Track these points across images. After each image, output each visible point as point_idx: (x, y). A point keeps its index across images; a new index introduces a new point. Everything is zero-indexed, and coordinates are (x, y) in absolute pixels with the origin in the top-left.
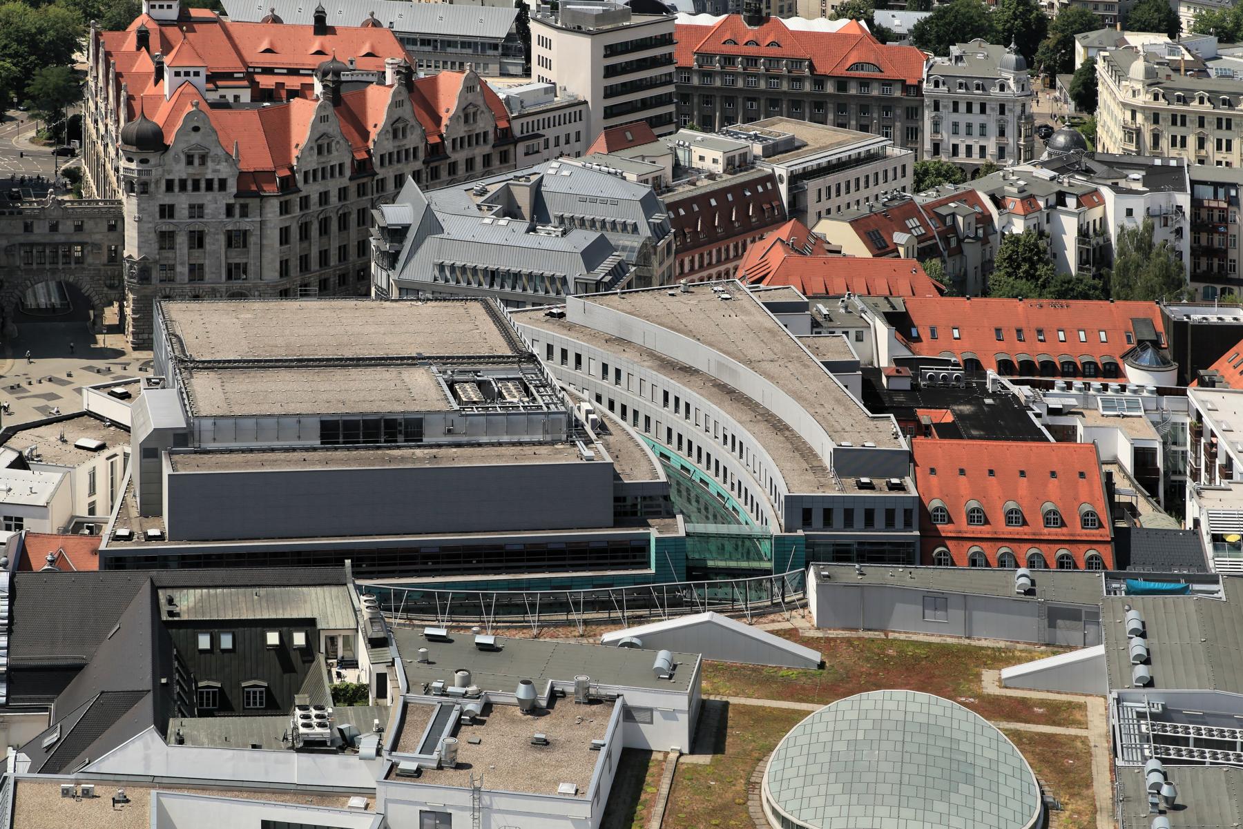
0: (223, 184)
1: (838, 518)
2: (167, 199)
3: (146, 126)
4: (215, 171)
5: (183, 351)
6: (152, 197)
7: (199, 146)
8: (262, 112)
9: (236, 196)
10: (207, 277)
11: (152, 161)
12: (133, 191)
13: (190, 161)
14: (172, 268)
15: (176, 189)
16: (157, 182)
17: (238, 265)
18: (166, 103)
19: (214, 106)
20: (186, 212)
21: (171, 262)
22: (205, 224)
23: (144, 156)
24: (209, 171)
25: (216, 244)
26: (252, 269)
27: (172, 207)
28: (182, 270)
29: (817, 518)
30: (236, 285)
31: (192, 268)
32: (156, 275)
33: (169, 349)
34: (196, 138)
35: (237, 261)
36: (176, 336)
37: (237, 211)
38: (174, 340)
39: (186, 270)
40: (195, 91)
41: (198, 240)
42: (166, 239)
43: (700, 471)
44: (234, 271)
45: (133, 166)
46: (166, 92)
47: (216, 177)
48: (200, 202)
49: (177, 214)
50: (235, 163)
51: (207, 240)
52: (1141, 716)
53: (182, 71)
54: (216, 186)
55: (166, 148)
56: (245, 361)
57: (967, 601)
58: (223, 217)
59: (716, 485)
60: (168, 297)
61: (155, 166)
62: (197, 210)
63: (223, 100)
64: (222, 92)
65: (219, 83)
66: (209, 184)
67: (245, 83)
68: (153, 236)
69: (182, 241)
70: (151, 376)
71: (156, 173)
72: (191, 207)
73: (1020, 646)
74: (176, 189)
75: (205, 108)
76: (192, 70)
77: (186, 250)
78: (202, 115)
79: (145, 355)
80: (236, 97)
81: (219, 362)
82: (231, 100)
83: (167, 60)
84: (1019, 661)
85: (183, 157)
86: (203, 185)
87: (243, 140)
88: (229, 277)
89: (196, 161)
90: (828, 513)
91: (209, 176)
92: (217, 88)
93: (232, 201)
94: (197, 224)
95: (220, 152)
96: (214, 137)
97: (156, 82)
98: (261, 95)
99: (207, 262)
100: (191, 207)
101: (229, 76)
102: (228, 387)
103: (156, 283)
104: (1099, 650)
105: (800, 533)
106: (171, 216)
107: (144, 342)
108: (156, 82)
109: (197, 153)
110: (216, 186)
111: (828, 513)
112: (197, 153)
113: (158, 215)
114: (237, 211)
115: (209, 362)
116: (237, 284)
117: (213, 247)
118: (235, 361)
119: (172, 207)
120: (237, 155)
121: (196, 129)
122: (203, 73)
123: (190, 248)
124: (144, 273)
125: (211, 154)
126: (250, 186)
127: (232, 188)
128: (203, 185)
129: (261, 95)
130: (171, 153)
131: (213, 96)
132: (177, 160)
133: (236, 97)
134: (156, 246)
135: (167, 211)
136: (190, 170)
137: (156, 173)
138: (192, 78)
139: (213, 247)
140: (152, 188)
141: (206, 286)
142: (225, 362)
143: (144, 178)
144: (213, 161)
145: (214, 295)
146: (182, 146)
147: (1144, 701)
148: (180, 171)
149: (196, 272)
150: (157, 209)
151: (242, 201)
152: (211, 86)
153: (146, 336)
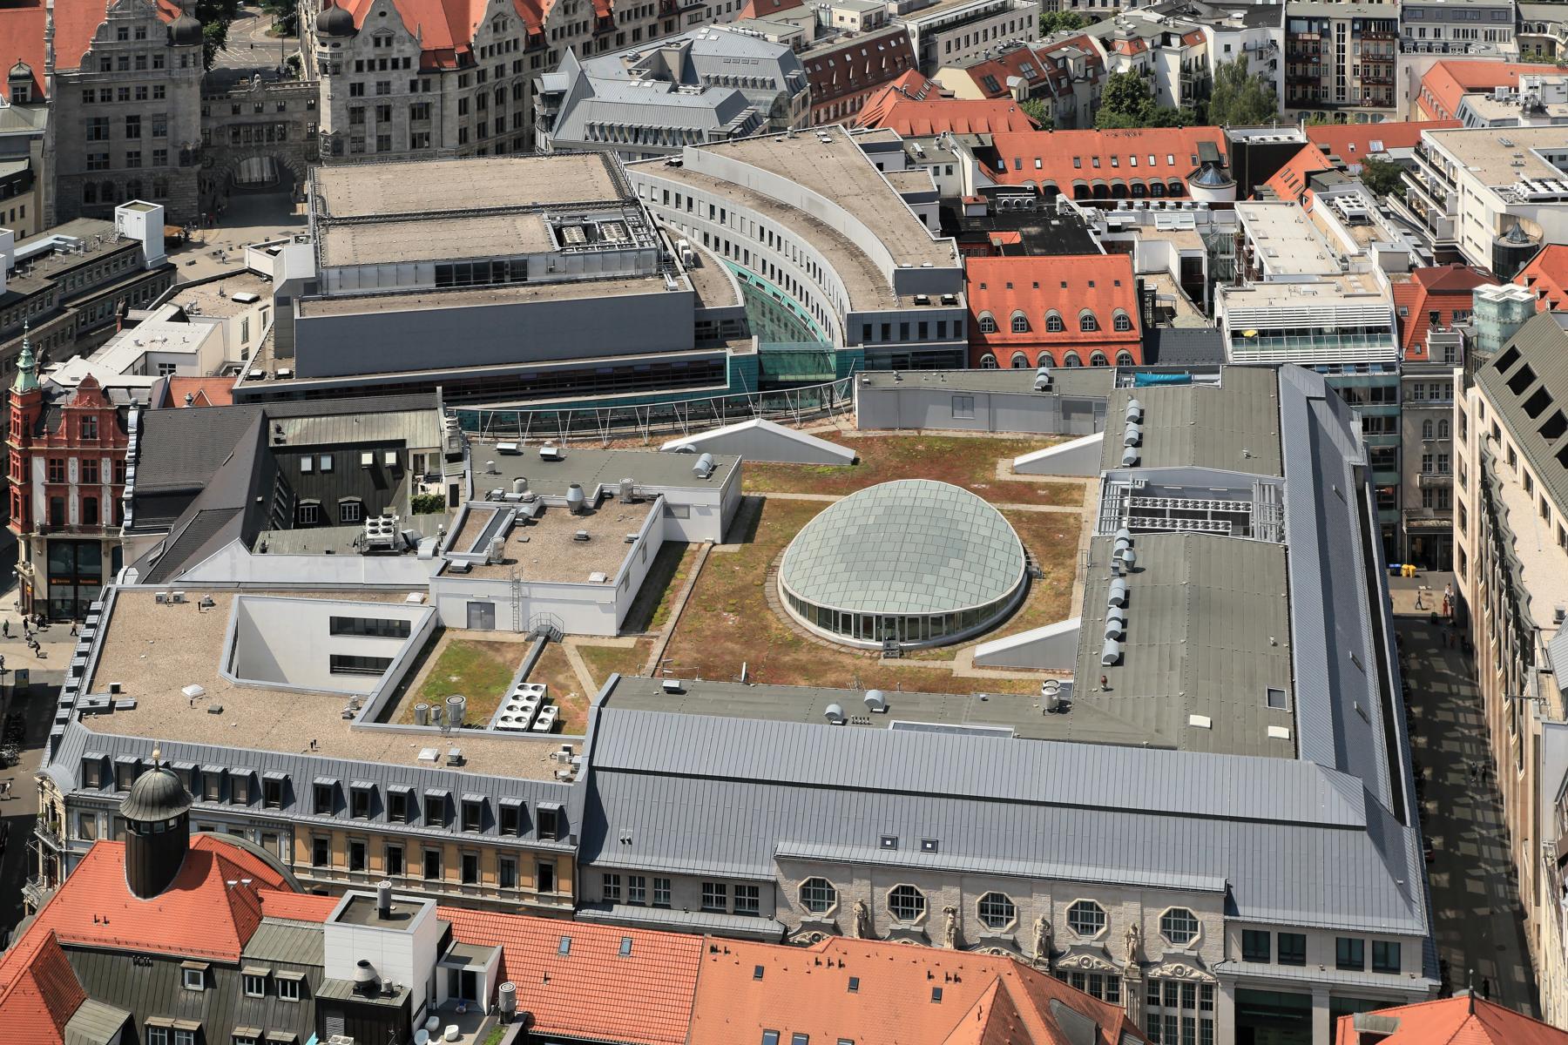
1: (895, 332)
26: (433, 138)
29: (877, 332)
43: (789, 297)
51: (394, 114)
52: (1125, 492)
57: (991, 400)
59: (801, 308)
69: (371, 116)
73: (1037, 437)
84: (1034, 449)
90: (886, 329)
104: (1099, 437)
105: (861, 346)
111: (886, 329)
147: (1130, 479)
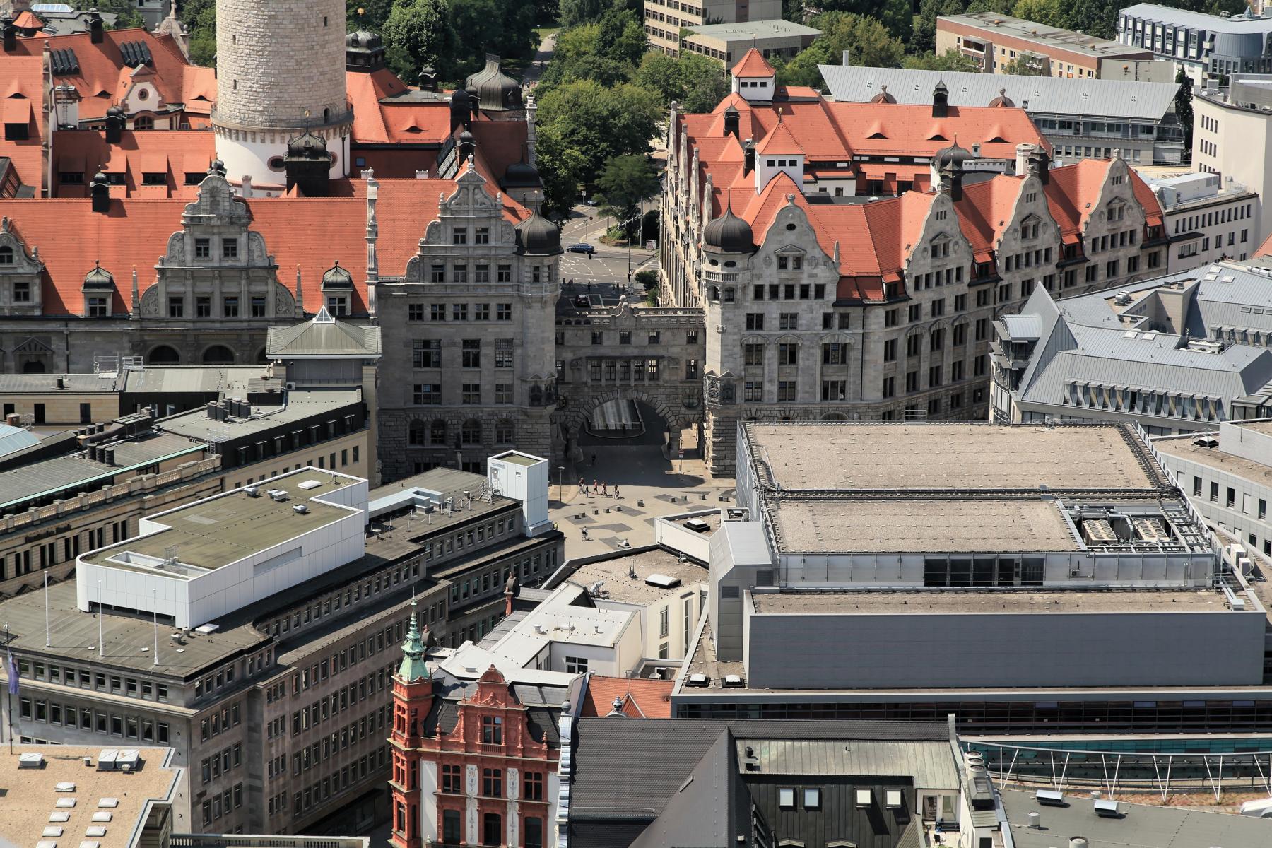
0: (820, 291)
2: (755, 308)
3: (734, 225)
4: (811, 276)
5: (770, 479)
6: (738, 306)
7: (793, 247)
8: (868, 207)
9: (834, 305)
10: (799, 396)
11: (740, 264)
12: (716, 298)
13: (783, 265)
14: (760, 386)
15: (767, 296)
16: (745, 288)
17: (834, 384)
18: (758, 197)
19: (812, 200)
20: (777, 323)
21: (759, 379)
22: (799, 336)
23: (730, 258)
24: (805, 276)
25: (810, 359)
27: (760, 317)
28: (771, 389)
30: (832, 406)
31: (782, 385)
32: (740, 393)
33: (754, 477)
34: (790, 237)
35: (834, 379)
36: (762, 463)
37: (836, 322)
38: (760, 467)
39: (775, 388)
40: (791, 183)
41: (789, 354)
42: (753, 353)
44: (830, 390)
45: (717, 269)
46: (758, 184)
47: (813, 283)
48: (793, 311)
49: (766, 325)
50: (835, 267)
53: (777, 159)
54: (812, 292)
55: (756, 249)
56: (840, 492)
58: (819, 328)
60: (754, 419)
61: (743, 269)
62: (789, 321)
63: (823, 194)
64: (821, 184)
65: (819, 174)
66: (805, 292)
67: (850, 174)
68: (738, 350)
70: (733, 507)
71: (743, 278)
72: (783, 316)
74: (767, 296)
75: (801, 201)
76: (788, 159)
77: (775, 366)
78: (798, 211)
79: (727, 483)
80: (839, 191)
81: (811, 492)
82: (832, 194)
83: (759, 147)
85: (775, 260)
86: (797, 292)
87: (845, 239)
88: (825, 396)
89: (790, 264)
91: (805, 282)
92: (817, 179)
93: (830, 310)
94: (789, 337)
95: (817, 253)
96: (812, 237)
97: (746, 173)
98: (869, 188)
99: (799, 379)
100: (783, 316)
101: (831, 165)
102: (821, 520)
103: (741, 402)
106: (760, 327)
107: (725, 469)
108: (746, 173)
109: (791, 255)
110: (812, 292)
112: (791, 255)
113: (744, 326)
114: (836, 322)
115: (799, 492)
116: (834, 404)
117: (807, 363)
118: (829, 492)
119: (760, 317)
120: (838, 258)
121: (791, 227)
122: (801, 162)
123: (781, 363)
124: (727, 392)
125: (808, 256)
126: (852, 293)
127: (831, 295)
128: (797, 292)
129: (869, 188)
130: (761, 255)
131: (812, 190)
132: (768, 263)
133: (839, 191)
134: (741, 361)
135: (755, 322)
136: (783, 274)
137: (743, 278)
138: (787, 168)
139: (807, 363)
140: (738, 295)
141: (797, 406)
142: (817, 492)
143: (730, 283)
144: (810, 264)
145: (806, 416)
146: (774, 247)
148: (771, 276)
149: (787, 390)
150: (744, 319)
151: (842, 310)
152: (810, 177)
153: (728, 462)
